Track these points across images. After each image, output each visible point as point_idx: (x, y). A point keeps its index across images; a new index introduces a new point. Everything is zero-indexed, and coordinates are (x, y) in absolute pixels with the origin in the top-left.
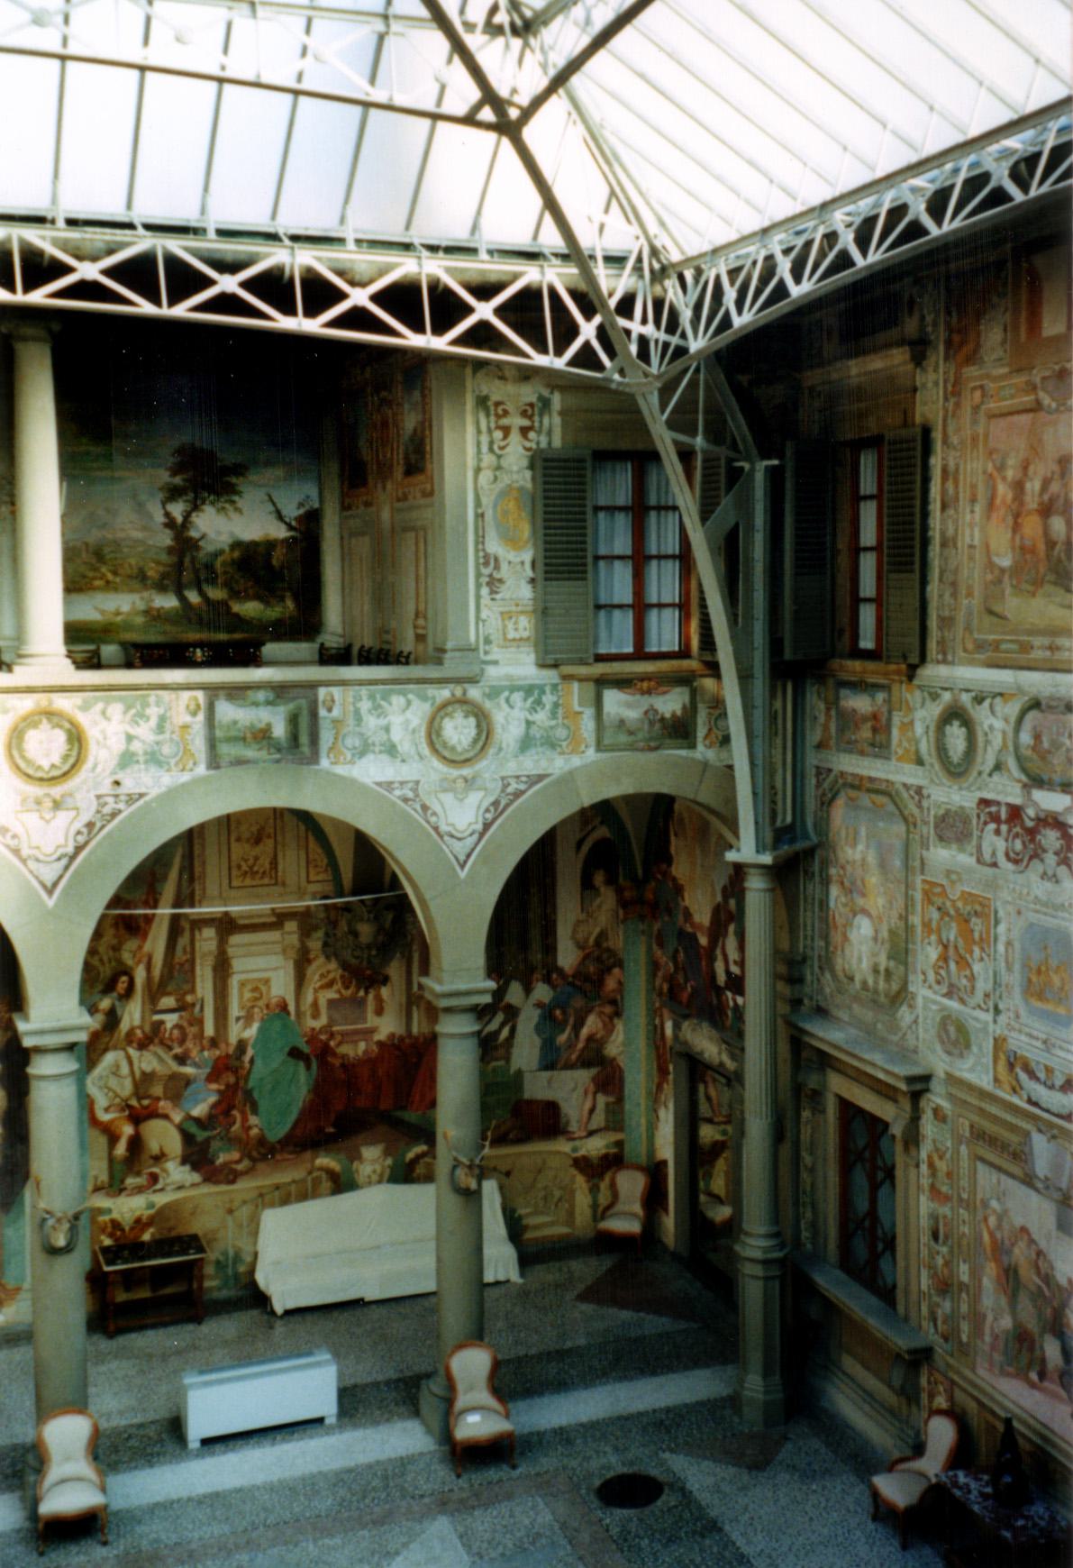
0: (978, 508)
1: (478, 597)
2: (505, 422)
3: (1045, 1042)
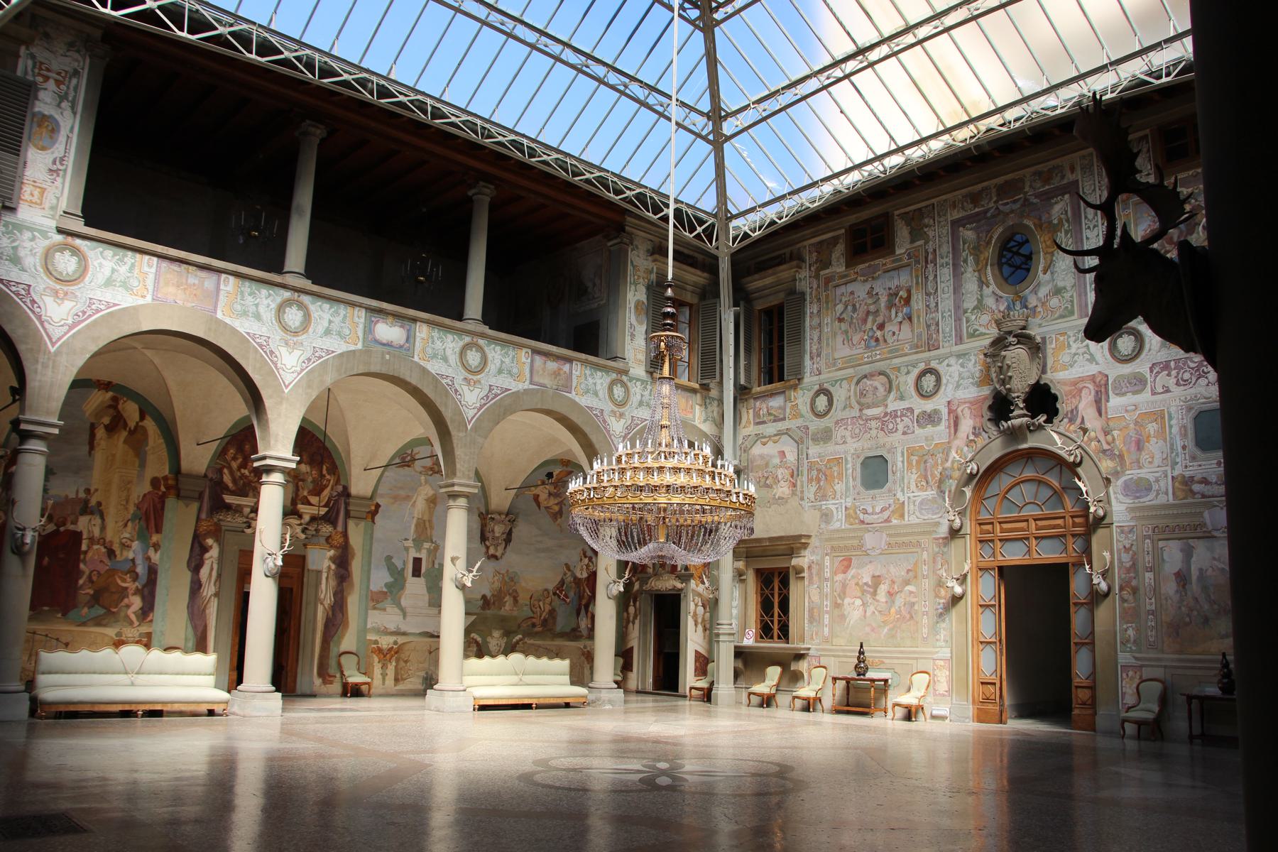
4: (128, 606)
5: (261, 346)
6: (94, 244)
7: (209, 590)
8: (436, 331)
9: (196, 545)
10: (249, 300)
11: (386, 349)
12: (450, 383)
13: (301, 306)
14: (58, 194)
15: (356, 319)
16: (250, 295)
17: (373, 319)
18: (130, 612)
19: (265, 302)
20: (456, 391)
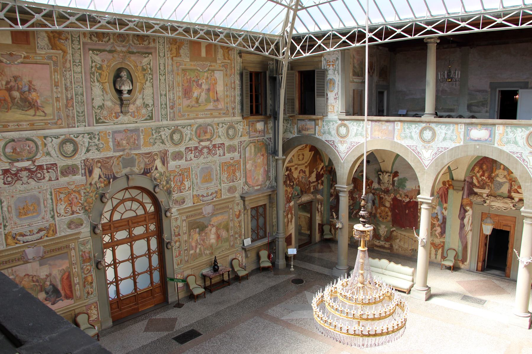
3: (29, 225)
4: (436, 231)
5: (413, 150)
6: (350, 121)
7: (468, 228)
8: (509, 128)
9: (462, 209)
10: (407, 131)
11: (477, 143)
12: (520, 156)
13: (431, 129)
14: (338, 105)
15: (460, 130)
16: (407, 129)
17: (469, 128)
18: (436, 233)
19: (414, 130)
20: (524, 160)
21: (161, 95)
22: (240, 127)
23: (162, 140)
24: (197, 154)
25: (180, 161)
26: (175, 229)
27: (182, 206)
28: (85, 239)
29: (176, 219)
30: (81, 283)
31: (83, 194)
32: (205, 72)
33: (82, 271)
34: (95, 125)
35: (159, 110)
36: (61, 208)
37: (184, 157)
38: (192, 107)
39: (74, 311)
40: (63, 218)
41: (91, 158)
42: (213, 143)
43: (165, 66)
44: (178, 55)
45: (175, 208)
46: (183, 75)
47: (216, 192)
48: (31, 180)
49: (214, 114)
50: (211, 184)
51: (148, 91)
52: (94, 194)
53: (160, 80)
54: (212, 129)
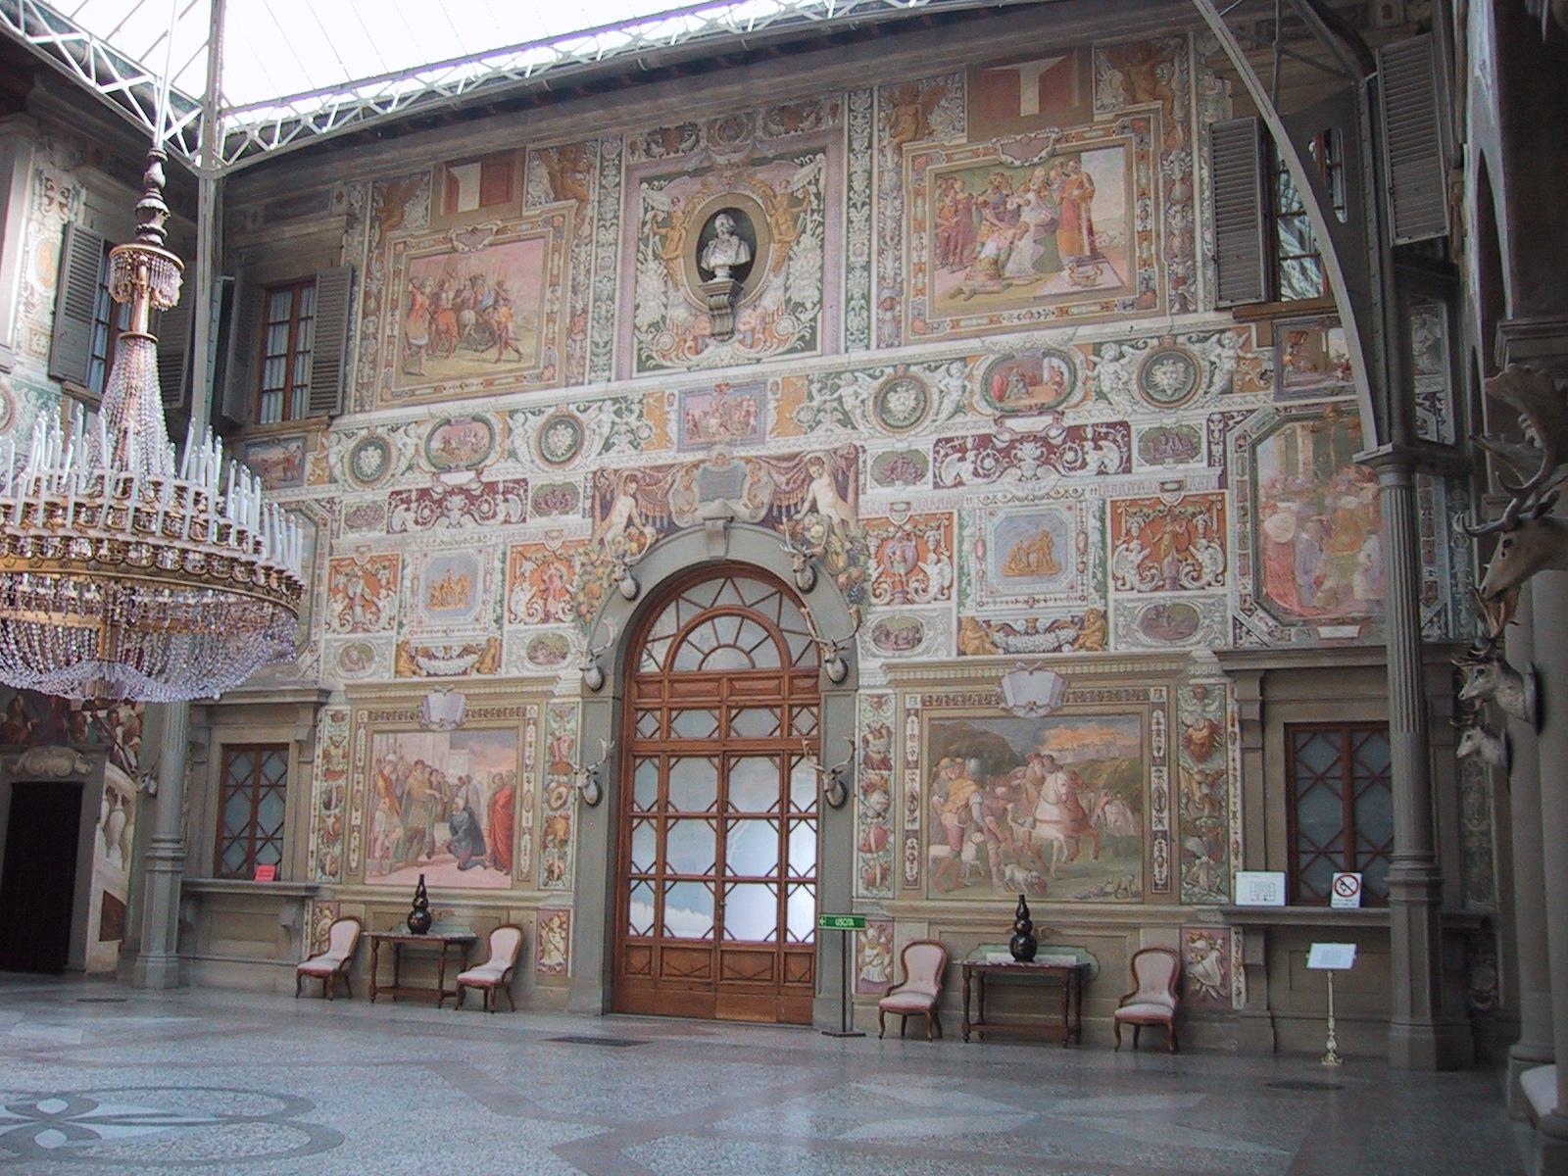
0: (397, 313)
1: (17, 311)
2: (50, 193)
21: (850, 269)
22: (1223, 356)
23: (845, 413)
24: (989, 463)
25: (911, 488)
26: (870, 737)
27: (906, 653)
28: (565, 700)
29: (880, 701)
30: (538, 833)
31: (578, 569)
32: (1035, 165)
33: (546, 795)
34: (635, 375)
35: (839, 316)
36: (521, 597)
37: (930, 475)
38: (974, 293)
39: (505, 914)
40: (522, 626)
41: (614, 466)
42: (1069, 421)
43: (870, 178)
44: (922, 130)
45: (874, 656)
46: (938, 192)
47: (1079, 623)
48: (468, 516)
49: (1075, 310)
50: (1051, 587)
51: (805, 260)
52: (607, 571)
53: (849, 222)
54: (1064, 368)
